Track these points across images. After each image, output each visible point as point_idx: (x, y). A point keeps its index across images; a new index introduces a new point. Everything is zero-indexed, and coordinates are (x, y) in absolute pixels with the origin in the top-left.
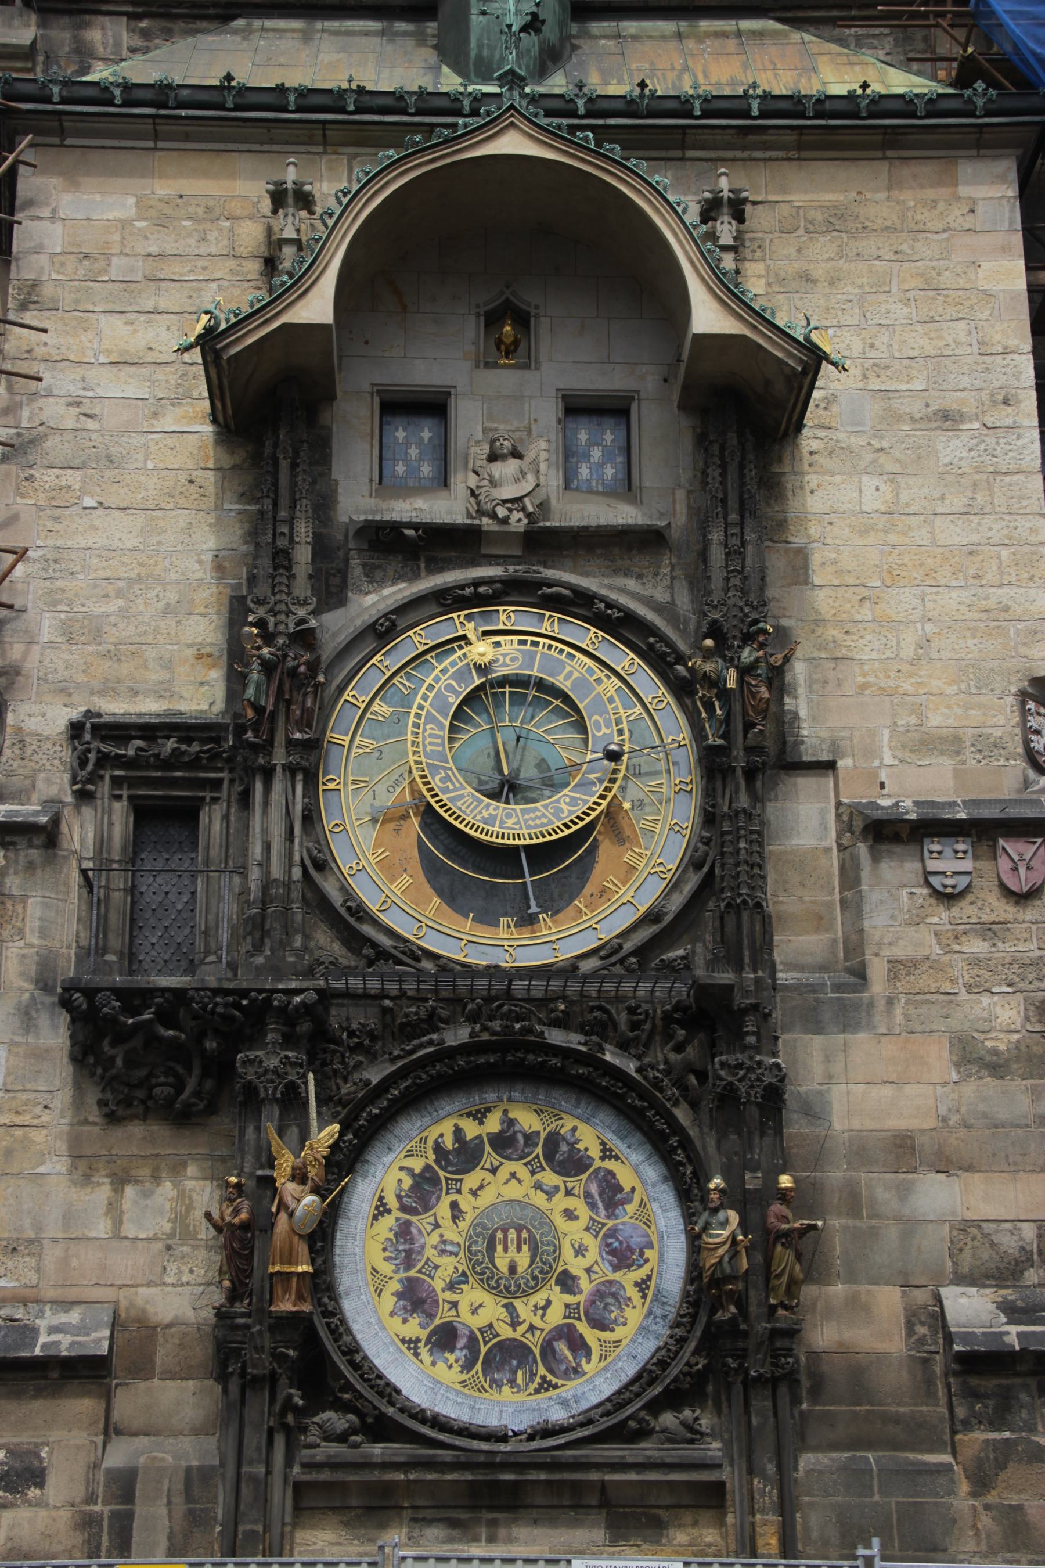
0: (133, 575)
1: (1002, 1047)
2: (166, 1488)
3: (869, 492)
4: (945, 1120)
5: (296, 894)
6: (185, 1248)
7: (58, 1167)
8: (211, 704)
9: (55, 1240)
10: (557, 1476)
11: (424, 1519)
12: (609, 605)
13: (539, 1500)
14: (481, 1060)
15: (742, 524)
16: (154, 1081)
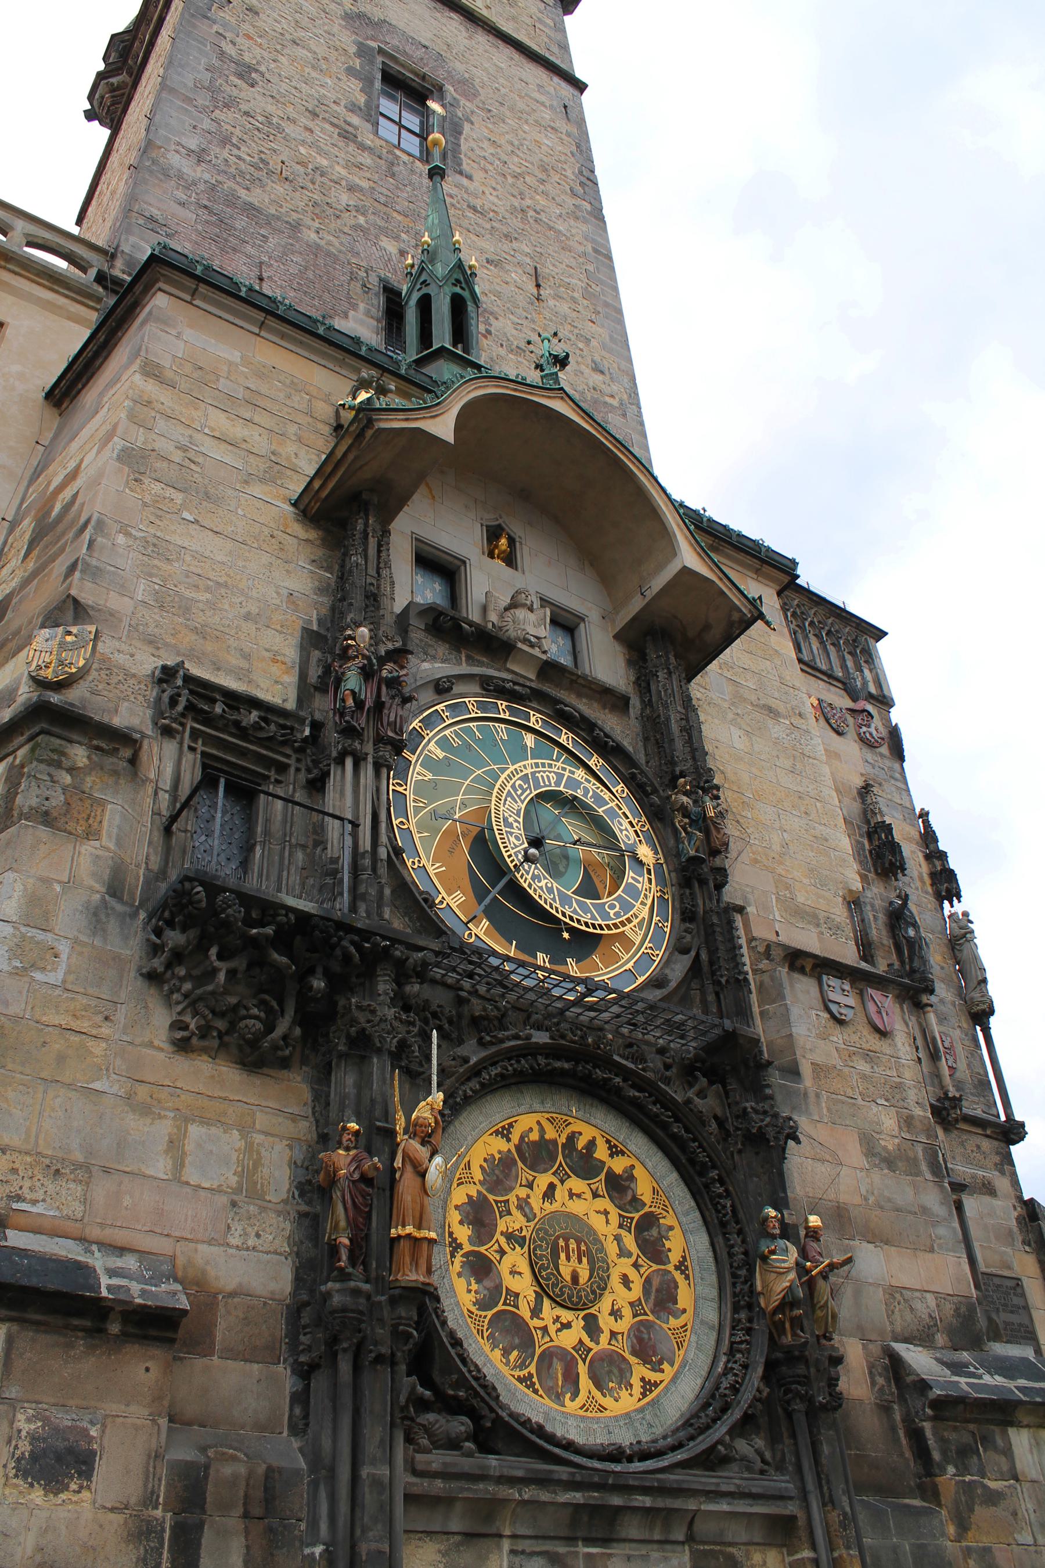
0: (220, 580)
1: (890, 1147)
2: (242, 1493)
3: (735, 737)
4: (866, 1199)
5: (383, 870)
6: (252, 1208)
7: (115, 1089)
8: (284, 701)
9: (107, 1171)
10: (660, 1503)
11: (523, 1552)
12: (607, 735)
13: (634, 1533)
14: (558, 1064)
15: (687, 715)
16: (243, 1012)
